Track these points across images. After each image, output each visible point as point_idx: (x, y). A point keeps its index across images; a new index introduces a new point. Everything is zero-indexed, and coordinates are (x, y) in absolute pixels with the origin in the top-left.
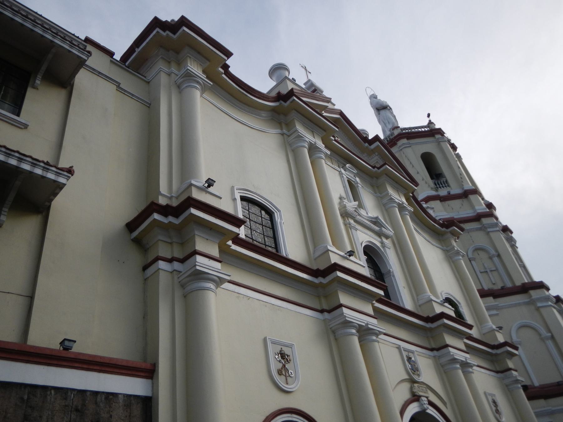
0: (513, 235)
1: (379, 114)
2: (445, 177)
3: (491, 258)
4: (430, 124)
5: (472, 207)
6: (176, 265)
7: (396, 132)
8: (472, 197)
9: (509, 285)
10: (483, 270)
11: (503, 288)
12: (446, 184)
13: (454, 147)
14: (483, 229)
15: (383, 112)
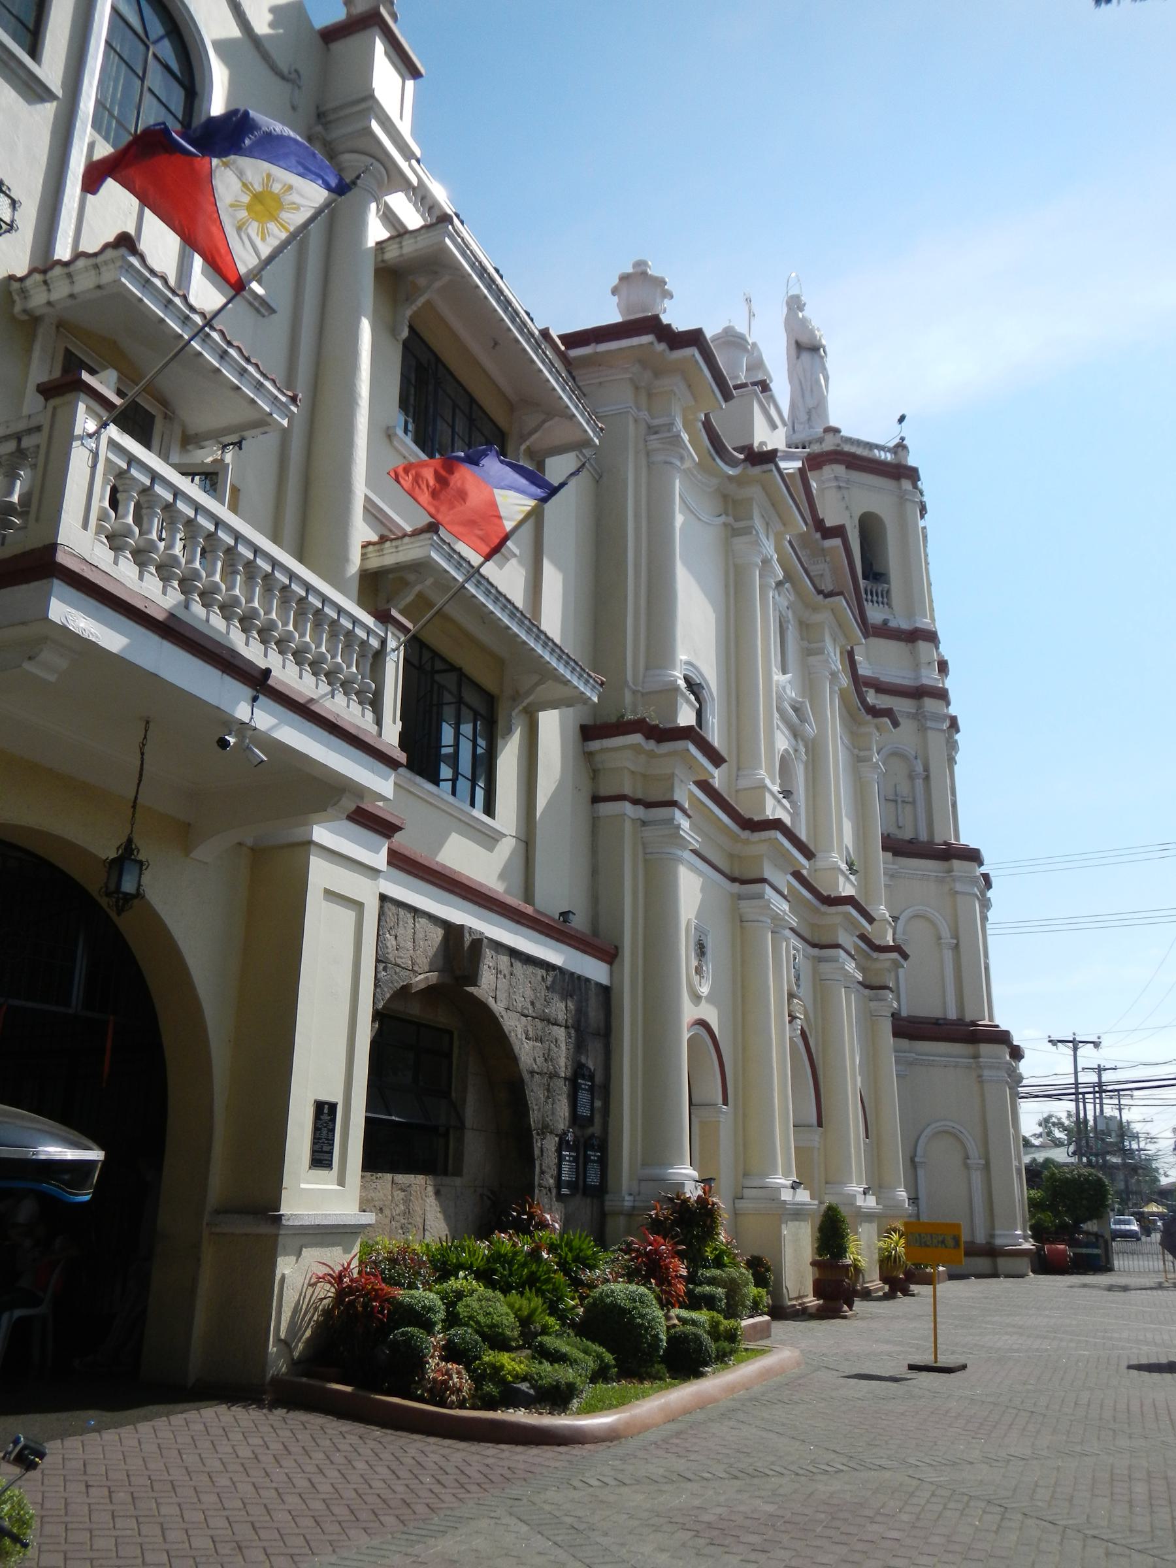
0: (958, 737)
1: (798, 358)
2: (887, 582)
3: (911, 777)
4: (900, 449)
5: (917, 666)
6: (639, 812)
7: (829, 445)
8: (922, 645)
9: (924, 837)
10: (891, 797)
11: (910, 842)
12: (884, 598)
13: (923, 510)
14: (919, 717)
15: (806, 356)
